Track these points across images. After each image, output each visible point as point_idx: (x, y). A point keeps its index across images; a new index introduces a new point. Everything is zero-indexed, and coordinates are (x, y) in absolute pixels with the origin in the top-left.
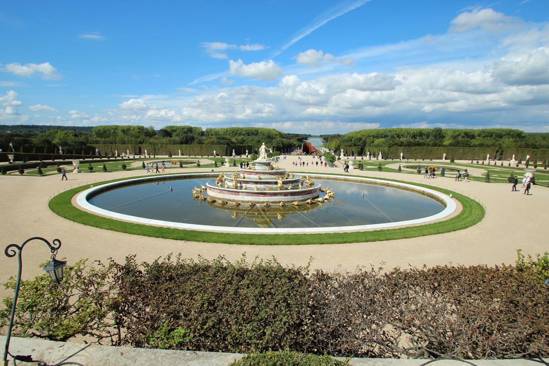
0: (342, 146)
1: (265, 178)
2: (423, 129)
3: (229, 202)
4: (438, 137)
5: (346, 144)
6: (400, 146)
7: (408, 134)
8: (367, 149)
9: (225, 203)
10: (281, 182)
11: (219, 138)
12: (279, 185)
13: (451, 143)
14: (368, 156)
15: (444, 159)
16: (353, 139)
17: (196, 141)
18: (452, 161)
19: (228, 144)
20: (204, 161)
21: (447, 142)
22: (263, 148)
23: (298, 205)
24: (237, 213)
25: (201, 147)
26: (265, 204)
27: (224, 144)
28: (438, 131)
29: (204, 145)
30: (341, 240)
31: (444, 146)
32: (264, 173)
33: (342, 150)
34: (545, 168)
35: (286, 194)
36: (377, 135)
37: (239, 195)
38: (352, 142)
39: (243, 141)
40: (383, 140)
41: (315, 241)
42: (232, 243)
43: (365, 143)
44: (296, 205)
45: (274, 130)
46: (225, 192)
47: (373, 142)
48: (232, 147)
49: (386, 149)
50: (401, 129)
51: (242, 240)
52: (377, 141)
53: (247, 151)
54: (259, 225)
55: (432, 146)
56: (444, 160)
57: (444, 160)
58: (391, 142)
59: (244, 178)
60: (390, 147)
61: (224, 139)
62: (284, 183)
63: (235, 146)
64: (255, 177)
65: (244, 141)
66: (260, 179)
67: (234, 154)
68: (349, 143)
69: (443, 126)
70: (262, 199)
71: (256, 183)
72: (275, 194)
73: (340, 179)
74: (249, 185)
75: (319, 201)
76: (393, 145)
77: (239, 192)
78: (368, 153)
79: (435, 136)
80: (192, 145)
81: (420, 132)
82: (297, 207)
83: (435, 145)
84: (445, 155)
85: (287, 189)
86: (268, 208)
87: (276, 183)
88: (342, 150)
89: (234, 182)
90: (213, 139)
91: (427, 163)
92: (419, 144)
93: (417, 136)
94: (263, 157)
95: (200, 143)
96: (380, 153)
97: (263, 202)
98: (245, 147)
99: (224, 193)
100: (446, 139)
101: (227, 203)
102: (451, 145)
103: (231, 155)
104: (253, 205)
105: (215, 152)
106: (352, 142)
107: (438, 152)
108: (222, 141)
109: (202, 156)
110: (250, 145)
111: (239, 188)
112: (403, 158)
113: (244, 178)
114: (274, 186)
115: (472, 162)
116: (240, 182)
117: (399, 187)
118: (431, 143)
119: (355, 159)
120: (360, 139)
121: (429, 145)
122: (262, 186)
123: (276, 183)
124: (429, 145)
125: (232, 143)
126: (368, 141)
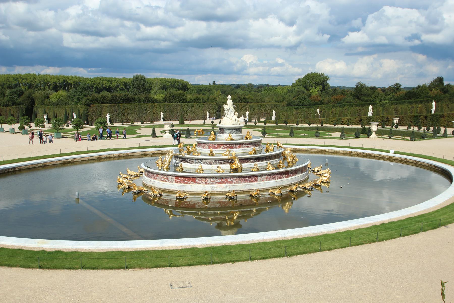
2: (68, 77)
4: (142, 89)
6: (103, 103)
7: (46, 84)
8: (38, 109)
13: (165, 98)
15: (162, 120)
16: (7, 92)
18: (182, 123)
28: (141, 80)
31: (156, 101)
34: (297, 125)
38: (6, 98)
40: (62, 93)
46: (233, 180)
47: (48, 98)
49: (82, 109)
50: (34, 75)
55: (144, 102)
60: (88, 105)
64: (220, 152)
79: (139, 88)
81: (64, 81)
84: (162, 114)
92: (128, 100)
94: (231, 118)
96: (75, 116)
99: (230, 182)
106: (6, 98)
107: (154, 111)
111: (240, 170)
115: (204, 123)
121: (140, 101)
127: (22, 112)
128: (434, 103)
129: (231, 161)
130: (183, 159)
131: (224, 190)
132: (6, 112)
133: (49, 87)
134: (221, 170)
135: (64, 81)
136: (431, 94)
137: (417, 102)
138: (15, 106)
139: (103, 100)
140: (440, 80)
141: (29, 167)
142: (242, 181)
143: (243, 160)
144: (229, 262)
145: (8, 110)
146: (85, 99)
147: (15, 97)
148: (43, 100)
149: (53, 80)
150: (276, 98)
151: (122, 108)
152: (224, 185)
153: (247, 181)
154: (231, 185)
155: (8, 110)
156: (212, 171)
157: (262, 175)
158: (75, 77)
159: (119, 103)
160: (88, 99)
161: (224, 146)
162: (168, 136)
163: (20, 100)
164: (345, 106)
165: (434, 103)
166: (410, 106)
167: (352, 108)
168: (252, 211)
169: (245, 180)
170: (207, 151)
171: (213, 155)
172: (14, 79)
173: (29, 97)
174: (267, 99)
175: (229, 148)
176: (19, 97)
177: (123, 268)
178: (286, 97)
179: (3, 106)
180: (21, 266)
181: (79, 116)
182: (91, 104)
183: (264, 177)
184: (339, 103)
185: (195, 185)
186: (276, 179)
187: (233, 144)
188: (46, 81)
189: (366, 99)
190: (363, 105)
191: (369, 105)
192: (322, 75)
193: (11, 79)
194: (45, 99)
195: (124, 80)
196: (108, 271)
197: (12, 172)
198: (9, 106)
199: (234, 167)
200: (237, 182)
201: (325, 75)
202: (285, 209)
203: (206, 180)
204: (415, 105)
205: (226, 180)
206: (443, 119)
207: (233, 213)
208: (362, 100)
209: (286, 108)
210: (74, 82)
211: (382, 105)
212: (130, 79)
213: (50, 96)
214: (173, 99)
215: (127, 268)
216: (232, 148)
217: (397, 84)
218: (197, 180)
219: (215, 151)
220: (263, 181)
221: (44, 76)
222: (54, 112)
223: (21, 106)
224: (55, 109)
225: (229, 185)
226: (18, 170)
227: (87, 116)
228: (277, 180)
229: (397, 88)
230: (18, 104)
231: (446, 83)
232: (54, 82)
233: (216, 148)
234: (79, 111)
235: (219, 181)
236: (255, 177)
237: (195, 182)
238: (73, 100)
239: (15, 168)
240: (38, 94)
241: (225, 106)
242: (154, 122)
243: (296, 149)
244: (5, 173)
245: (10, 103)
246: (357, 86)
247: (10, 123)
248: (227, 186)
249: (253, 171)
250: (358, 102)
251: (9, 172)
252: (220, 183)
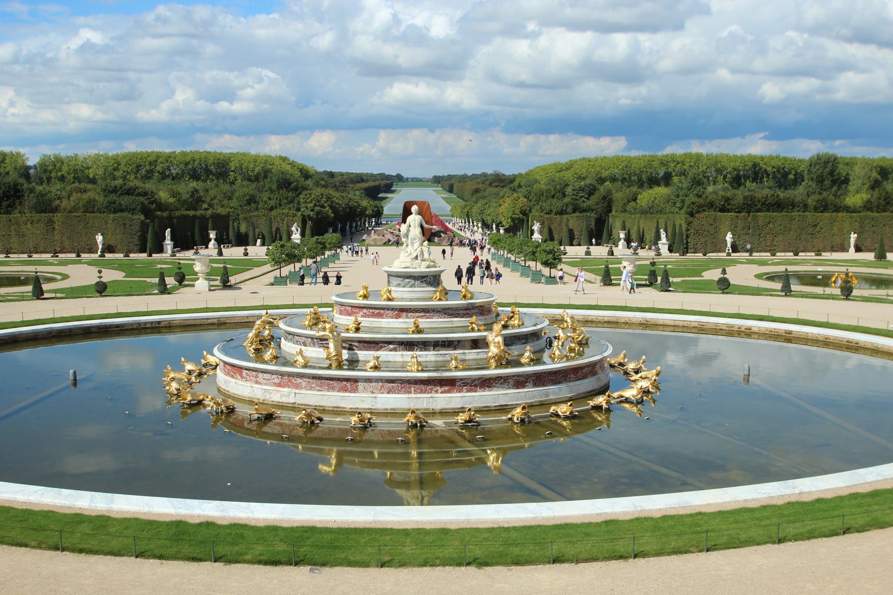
0: (535, 213)
1: (434, 327)
2: (762, 158)
3: (326, 418)
4: (827, 183)
5: (546, 206)
6: (723, 210)
7: (719, 171)
8: (615, 221)
9: (312, 421)
10: (500, 339)
11: (114, 190)
12: (493, 350)
13: (869, 201)
14: (622, 243)
16: (569, 190)
17: (30, 200)
19: (146, 211)
20: (83, 273)
21: (855, 198)
23: (571, 417)
24: (340, 455)
25: (51, 222)
26: (461, 418)
27: (133, 211)
28: (826, 163)
29: (58, 217)
30: (827, 525)
31: (848, 209)
32: (426, 311)
33: (536, 227)
35: (520, 382)
36: (656, 176)
37: (355, 390)
38: (567, 200)
39: (195, 201)
40: (661, 191)
41: (753, 533)
42: (487, 564)
43: (608, 204)
44: (566, 418)
45: (284, 159)
46: (303, 382)
47: (635, 200)
48: (161, 219)
49: (681, 220)
50: (698, 157)
51: (516, 551)
52: (646, 196)
53: (212, 235)
54: (400, 492)
55: (816, 209)
56: (851, 254)
57: (851, 254)
58: (692, 198)
59: (357, 330)
60: (692, 214)
61: (129, 192)
62: (509, 341)
63: (170, 218)
65: (200, 200)
66: (420, 331)
67: (168, 244)
68: (557, 204)
69: (842, 149)
70: (442, 399)
71: (409, 345)
72: (486, 383)
73: (628, 324)
74: (385, 355)
75: (627, 400)
76: (701, 208)
77: (355, 380)
78: (622, 235)
79: (820, 180)
80: (15, 215)
81: (755, 165)
82: (564, 423)
83: (823, 207)
84: (853, 237)
85: (519, 364)
86: (474, 429)
87: (476, 344)
88: (536, 227)
89: (331, 345)
90: (90, 195)
91: (807, 262)
92: (778, 206)
93: (746, 177)
95: (46, 207)
96: (663, 235)
97: (456, 412)
98: (203, 219)
99: (297, 386)
100: (852, 188)
101: (321, 419)
102: (868, 206)
103: (161, 250)
104: (419, 426)
105: (99, 238)
106: (567, 200)
107: (835, 230)
108: (125, 200)
109: (55, 253)
110: (222, 211)
112: (735, 249)
113: (357, 330)
114: (472, 354)
116: (350, 345)
117: (826, 343)
118: (811, 201)
119: (588, 253)
120: (591, 191)
121: (806, 207)
122: (429, 356)
123: (476, 344)
124: (806, 207)
125: (161, 206)
126: (619, 195)
127: (588, 226)
131: (285, 400)
132: (560, 225)
133: (725, 178)
134: (300, 359)
135: (755, 165)
138: (577, 214)
139: (723, 205)
141: (188, 323)
142: (321, 386)
145: (565, 221)
147: (582, 197)
148: (625, 204)
149: (732, 164)
151: (761, 222)
152: (286, 390)
153: (333, 389)
154: (297, 391)
155: (565, 221)
157: (369, 380)
158: (778, 157)
159: (759, 211)
160: (693, 203)
161: (365, 310)
168: (372, 453)
169: (328, 385)
172: (661, 163)
173: (604, 198)
175: (374, 315)
176: (588, 199)
179: (556, 214)
182: (699, 212)
183: (374, 384)
185: (240, 382)
186: (411, 392)
187: (384, 309)
188: (719, 166)
193: (656, 164)
194: (629, 202)
195: (880, 163)
197: (152, 328)
198: (567, 213)
200: (311, 389)
203: (257, 377)
205: (290, 381)
207: (329, 453)
210: (774, 167)
213: (639, 196)
214: (888, 203)
216: (380, 316)
220: (372, 392)
221: (717, 156)
222: (639, 227)
223: (588, 214)
224: (641, 222)
225: (294, 391)
226: (166, 327)
227: (687, 236)
228: (413, 395)
230: (585, 211)
232: (735, 169)
233: (350, 315)
234: (674, 225)
235: (277, 381)
237: (242, 377)
238: (675, 204)
239: (159, 322)
242: (823, 254)
243: (790, 332)
244: (137, 329)
245: (569, 209)
248: (289, 393)
249: (366, 370)
251: (146, 328)
252: (279, 385)
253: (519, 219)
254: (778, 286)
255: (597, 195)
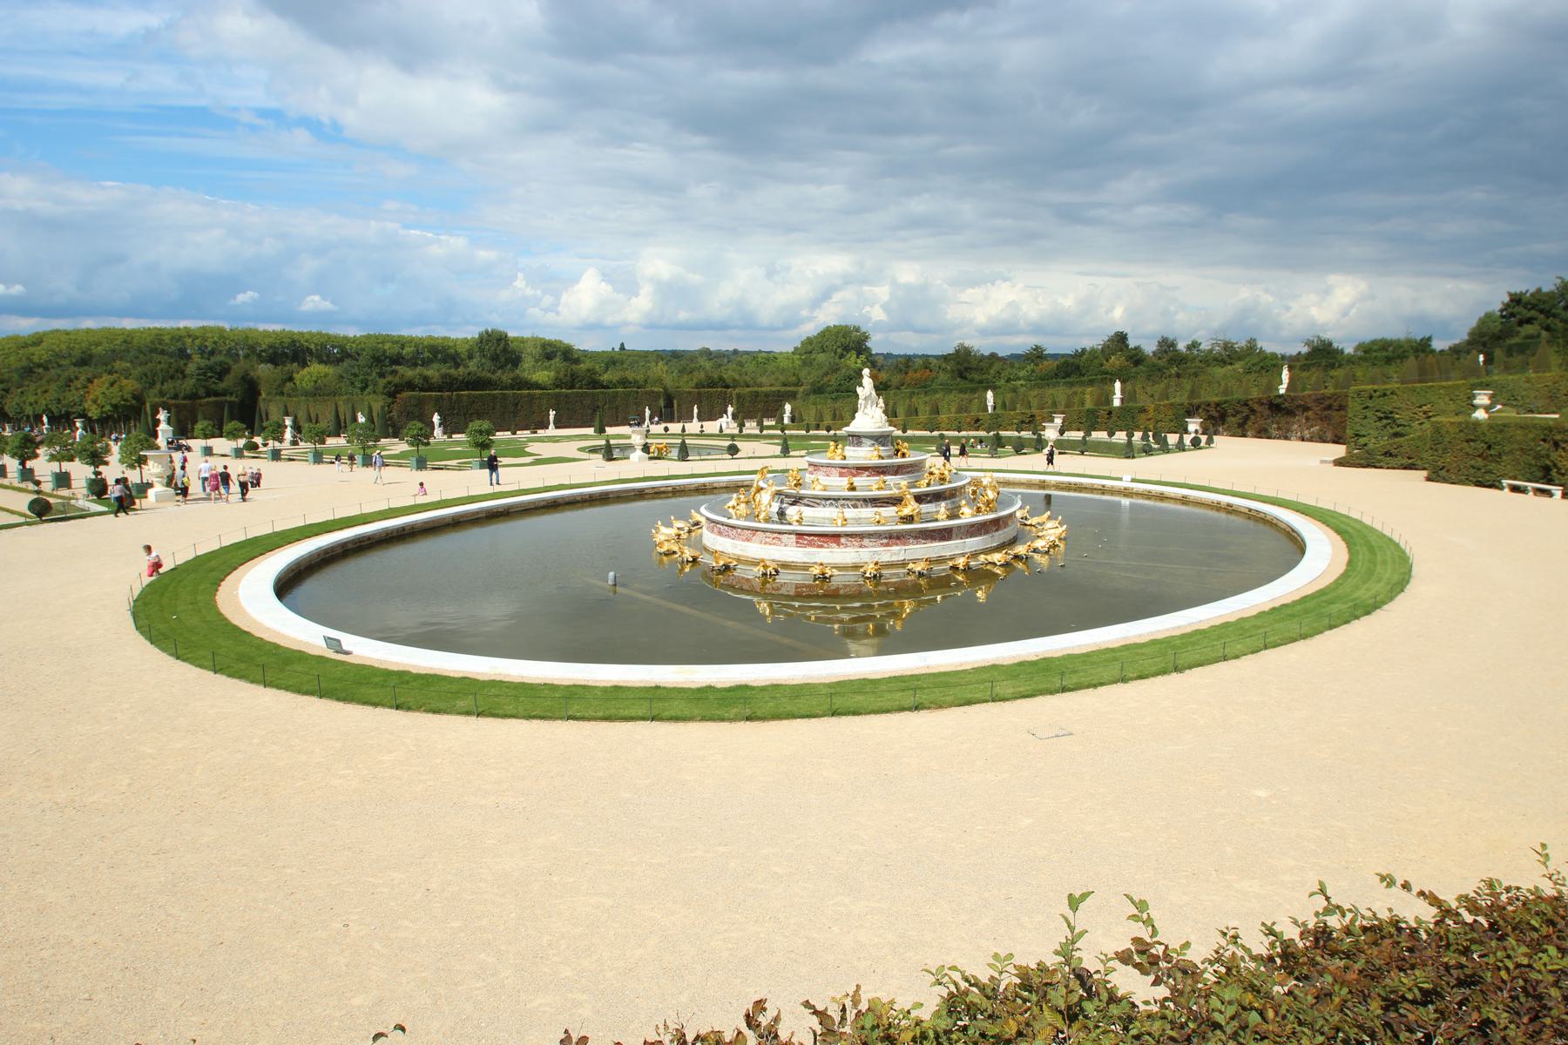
0: (152, 397)
8: (270, 406)
15: (552, 425)
18: (601, 431)
22: (866, 388)
31: (537, 386)
37: (949, 539)
47: (291, 379)
56: (552, 431)
57: (552, 431)
60: (392, 395)
78: (288, 421)
79: (495, 358)
84: (552, 413)
94: (870, 416)
96: (361, 419)
128: (1118, 385)
129: (896, 501)
130: (797, 500)
131: (895, 558)
136: (1107, 366)
137: (1082, 384)
140: (1121, 338)
143: (919, 499)
144: (1088, 687)
146: (382, 382)
150: (782, 379)
152: (895, 548)
156: (858, 521)
162: (637, 455)
163: (222, 386)
164: (936, 391)
165: (1118, 385)
166: (1070, 391)
167: (951, 396)
170: (845, 482)
171: (853, 489)
174: (764, 380)
177: (910, 709)
178: (803, 374)
180: (704, 719)
181: (370, 419)
184: (924, 387)
189: (976, 376)
190: (973, 390)
191: (986, 389)
192: (857, 329)
196: (884, 717)
199: (906, 511)
201: (863, 330)
202: (979, 594)
204: (1078, 389)
206: (1143, 416)
208: (972, 381)
209: (812, 397)
211: (1014, 390)
212: (466, 341)
215: (917, 708)
217: (1037, 348)
218: (843, 540)
219: (857, 481)
229: (1037, 355)
231: (1132, 343)
236: (835, 537)
240: (264, 370)
241: (859, 390)
246: (957, 352)
247: (712, 416)
250: (964, 384)
252: (887, 545)
253: (132, 406)
254: (777, 450)
255: (232, 375)
